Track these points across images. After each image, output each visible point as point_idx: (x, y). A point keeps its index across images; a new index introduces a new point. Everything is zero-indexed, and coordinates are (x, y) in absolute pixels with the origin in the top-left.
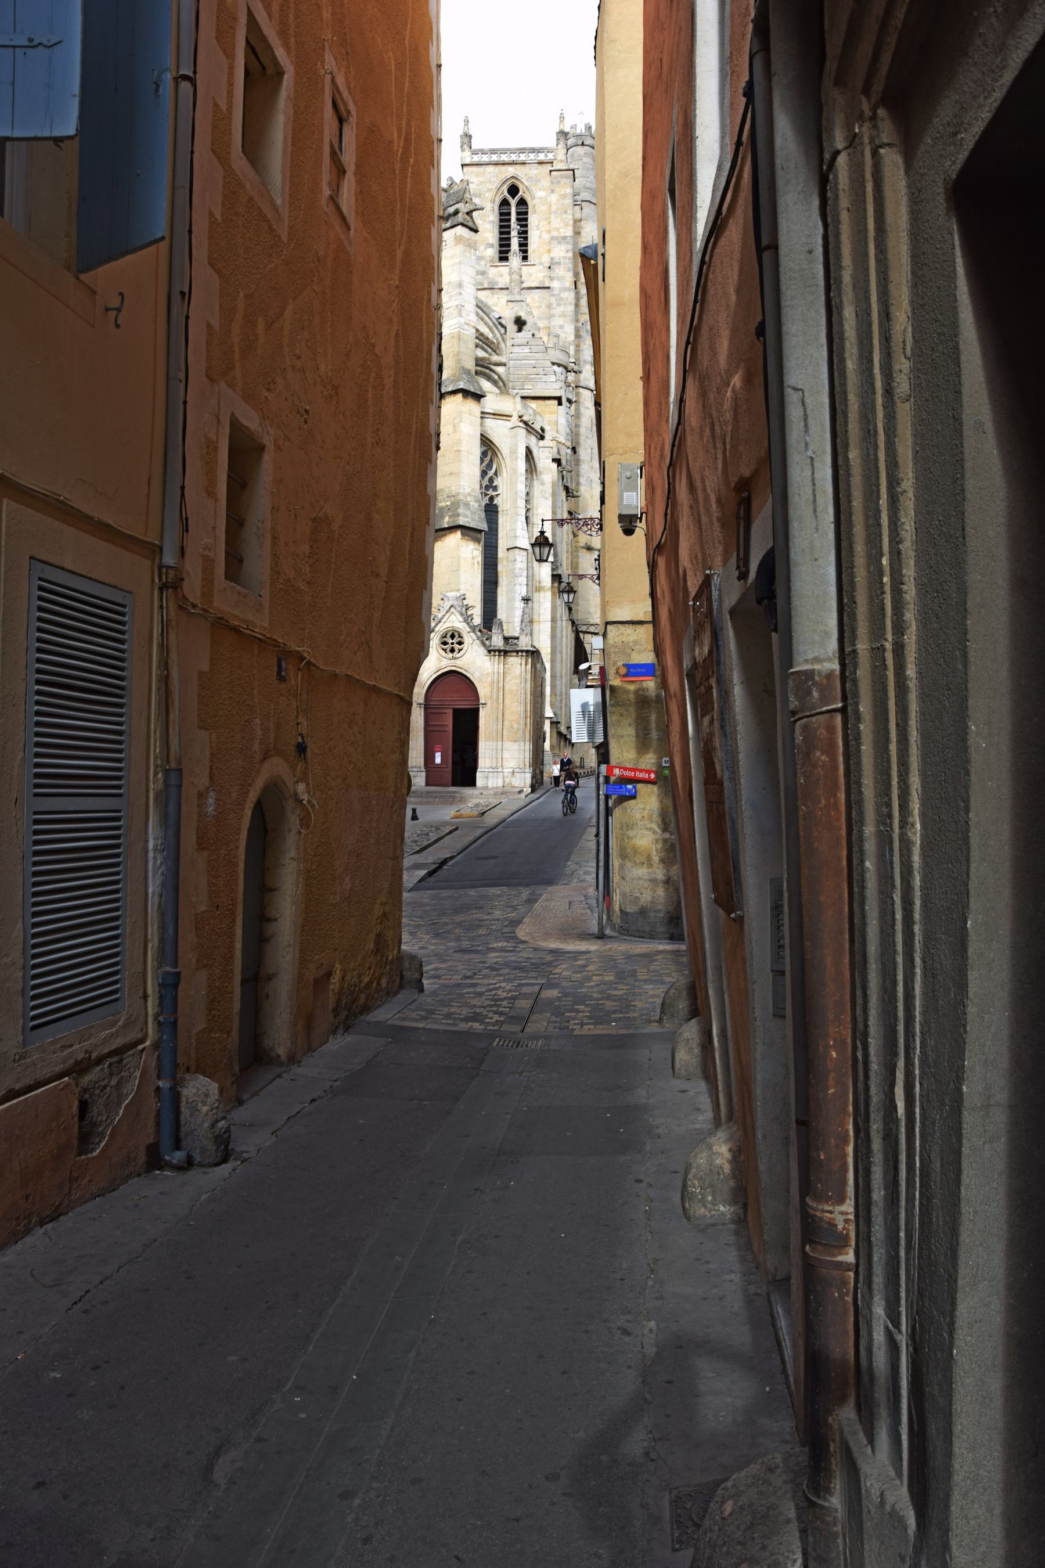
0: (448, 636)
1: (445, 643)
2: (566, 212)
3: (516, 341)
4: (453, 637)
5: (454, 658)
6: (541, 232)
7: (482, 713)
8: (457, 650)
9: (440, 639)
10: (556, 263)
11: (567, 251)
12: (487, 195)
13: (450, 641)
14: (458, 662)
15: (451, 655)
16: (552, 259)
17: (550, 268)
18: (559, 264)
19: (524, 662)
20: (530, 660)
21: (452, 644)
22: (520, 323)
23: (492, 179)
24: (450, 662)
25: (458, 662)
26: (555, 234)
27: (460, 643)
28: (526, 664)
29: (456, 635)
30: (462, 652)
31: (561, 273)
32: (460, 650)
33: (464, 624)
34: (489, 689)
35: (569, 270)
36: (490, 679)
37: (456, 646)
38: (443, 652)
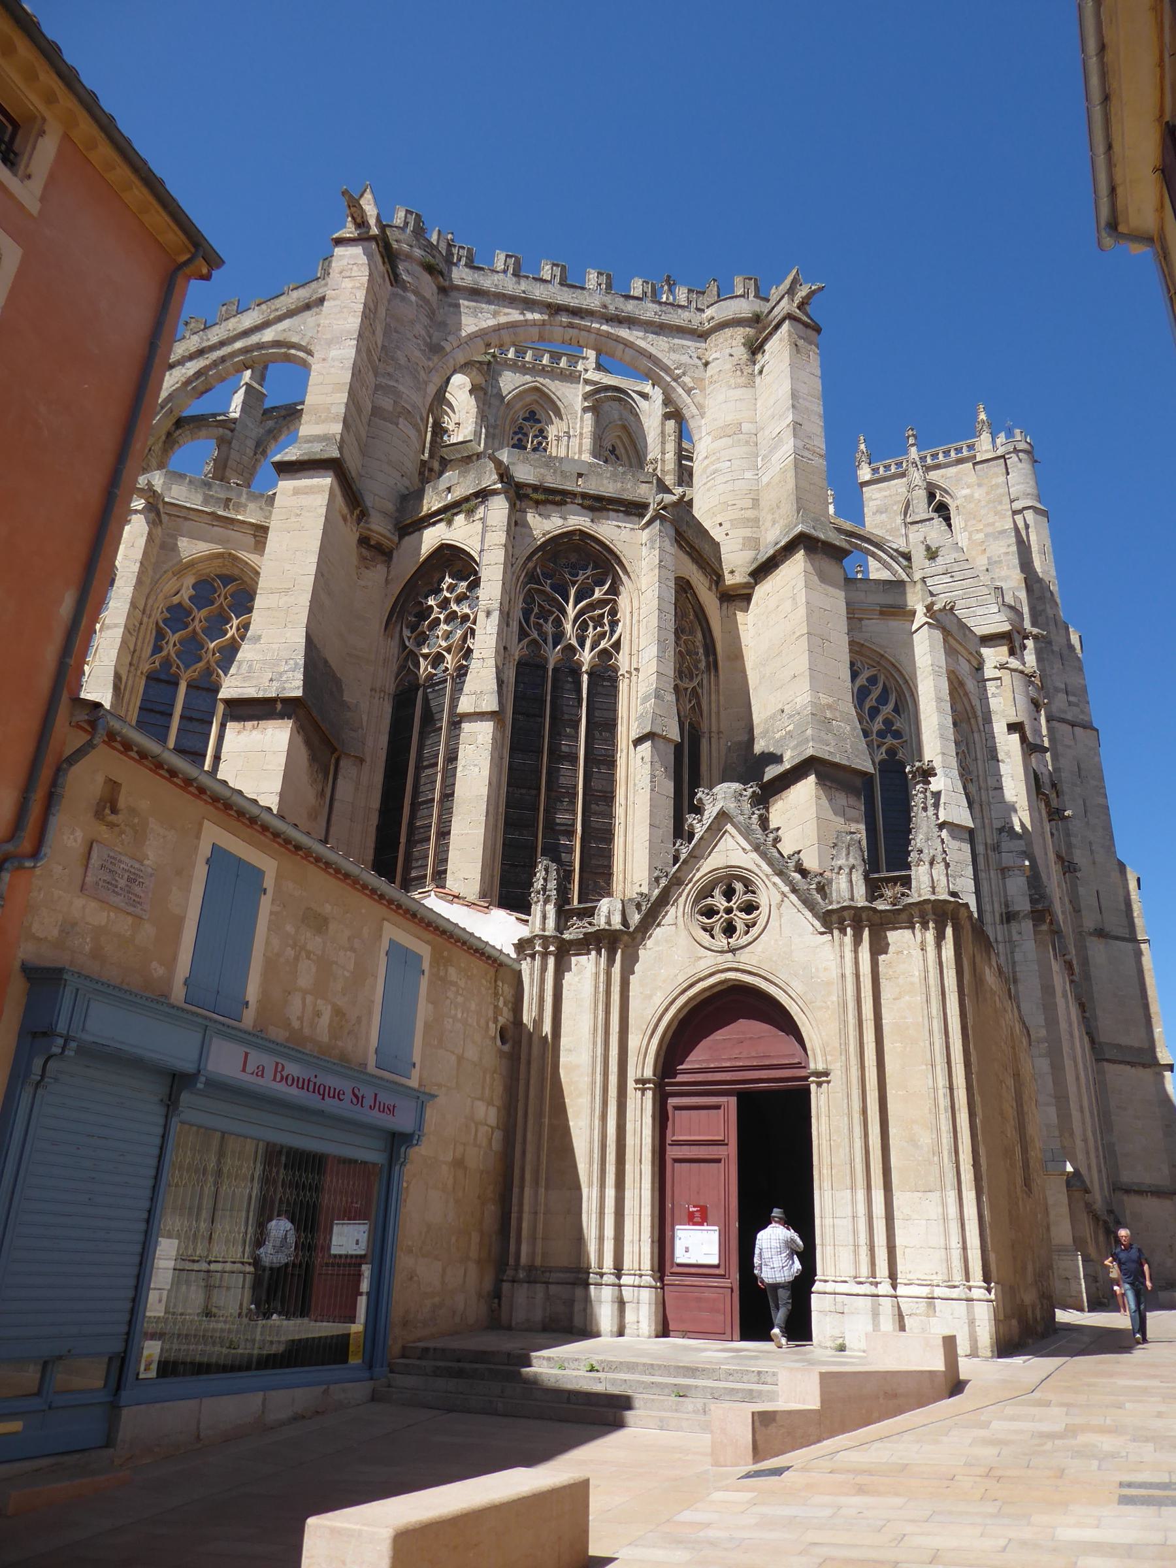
0: (717, 892)
1: (710, 912)
2: (1000, 503)
3: (929, 572)
4: (729, 894)
5: (733, 951)
6: (970, 534)
7: (819, 1100)
8: (740, 926)
9: (697, 901)
10: (996, 562)
11: (1009, 546)
12: (895, 508)
13: (719, 902)
14: (746, 958)
15: (722, 941)
16: (989, 558)
17: (987, 570)
18: (1000, 562)
19: (930, 935)
20: (949, 931)
21: (729, 911)
22: (932, 554)
23: (899, 490)
24: (721, 958)
25: (746, 958)
26: (990, 530)
27: (750, 908)
28: (939, 946)
29: (739, 886)
30: (754, 931)
31: (1003, 573)
32: (749, 926)
33: (755, 855)
34: (834, 1026)
35: (1014, 567)
36: (835, 998)
37: (740, 918)
38: (705, 937)
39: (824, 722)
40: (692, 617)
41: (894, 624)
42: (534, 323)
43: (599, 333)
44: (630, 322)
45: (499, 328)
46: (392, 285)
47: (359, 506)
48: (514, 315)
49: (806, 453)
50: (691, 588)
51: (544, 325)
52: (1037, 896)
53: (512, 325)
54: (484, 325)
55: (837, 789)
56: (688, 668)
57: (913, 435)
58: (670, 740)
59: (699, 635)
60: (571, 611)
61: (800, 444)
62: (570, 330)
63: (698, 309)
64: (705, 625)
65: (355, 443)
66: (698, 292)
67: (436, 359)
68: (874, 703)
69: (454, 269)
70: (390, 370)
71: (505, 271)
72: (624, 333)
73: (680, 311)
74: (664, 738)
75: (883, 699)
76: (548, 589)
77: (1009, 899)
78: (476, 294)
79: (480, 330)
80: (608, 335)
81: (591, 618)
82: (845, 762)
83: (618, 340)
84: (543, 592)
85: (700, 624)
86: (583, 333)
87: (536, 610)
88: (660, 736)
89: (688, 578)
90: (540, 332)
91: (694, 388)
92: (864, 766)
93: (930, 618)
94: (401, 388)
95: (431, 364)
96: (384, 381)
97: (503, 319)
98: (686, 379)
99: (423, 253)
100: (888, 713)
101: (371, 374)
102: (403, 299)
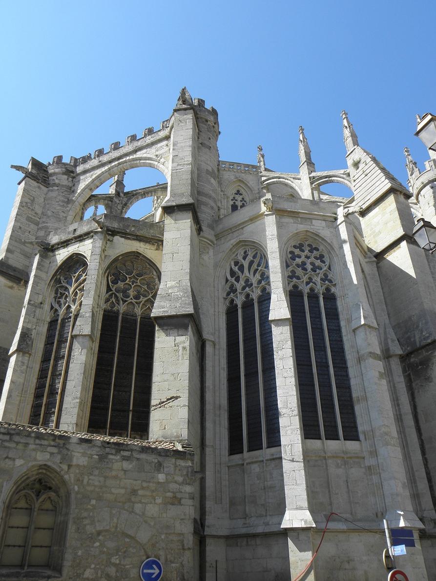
39: (165, 296)
40: (148, 266)
41: (258, 223)
42: (106, 171)
43: (130, 161)
44: (140, 149)
45: (93, 180)
46: (48, 188)
47: (22, 280)
48: (98, 172)
49: (180, 167)
50: (141, 254)
51: (110, 170)
52: (428, 335)
53: (98, 177)
54: (87, 183)
55: (171, 329)
56: (145, 290)
57: (344, 114)
58: (85, 335)
59: (155, 273)
60: (71, 290)
61: (175, 164)
62: (119, 166)
63: (166, 127)
64: (155, 268)
65: (23, 257)
66: (167, 121)
67: (70, 206)
68: (256, 267)
69: (78, 168)
70: (44, 220)
71: (95, 158)
72: (139, 154)
73: (159, 133)
74: (82, 335)
75: (259, 265)
76: (64, 284)
77: (359, 348)
78: (85, 172)
79: (86, 185)
80: (134, 160)
81: (79, 290)
82: (173, 313)
83: (136, 159)
84: (63, 286)
85: (154, 269)
86: (125, 164)
87: (59, 295)
88: (79, 335)
89: (136, 250)
90: (109, 174)
91: (165, 162)
92: (187, 311)
93: (270, 211)
94: (48, 225)
95: (68, 208)
96: (40, 226)
97: (94, 177)
98: (162, 160)
99: (60, 169)
100: (261, 270)
101: (32, 226)
102: (52, 191)
